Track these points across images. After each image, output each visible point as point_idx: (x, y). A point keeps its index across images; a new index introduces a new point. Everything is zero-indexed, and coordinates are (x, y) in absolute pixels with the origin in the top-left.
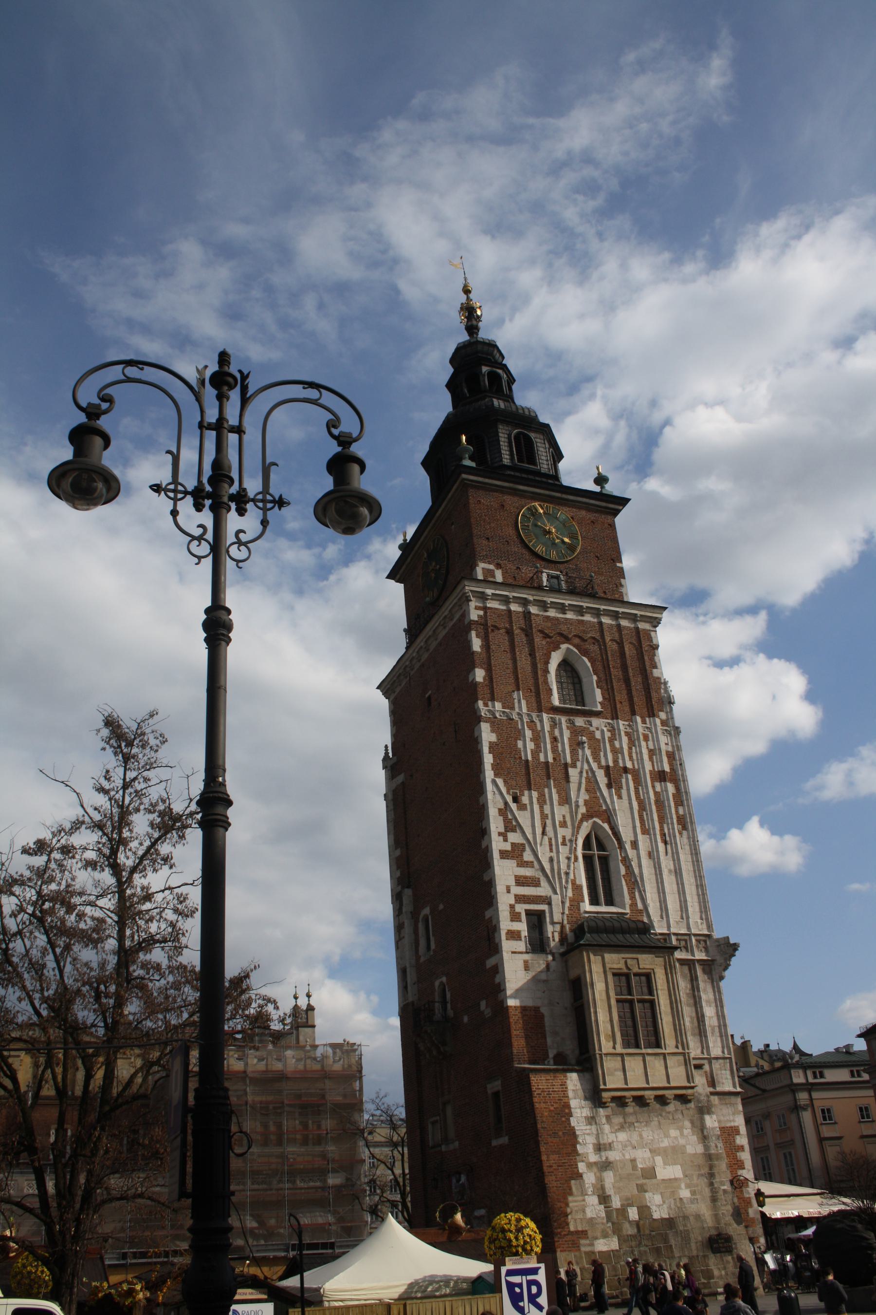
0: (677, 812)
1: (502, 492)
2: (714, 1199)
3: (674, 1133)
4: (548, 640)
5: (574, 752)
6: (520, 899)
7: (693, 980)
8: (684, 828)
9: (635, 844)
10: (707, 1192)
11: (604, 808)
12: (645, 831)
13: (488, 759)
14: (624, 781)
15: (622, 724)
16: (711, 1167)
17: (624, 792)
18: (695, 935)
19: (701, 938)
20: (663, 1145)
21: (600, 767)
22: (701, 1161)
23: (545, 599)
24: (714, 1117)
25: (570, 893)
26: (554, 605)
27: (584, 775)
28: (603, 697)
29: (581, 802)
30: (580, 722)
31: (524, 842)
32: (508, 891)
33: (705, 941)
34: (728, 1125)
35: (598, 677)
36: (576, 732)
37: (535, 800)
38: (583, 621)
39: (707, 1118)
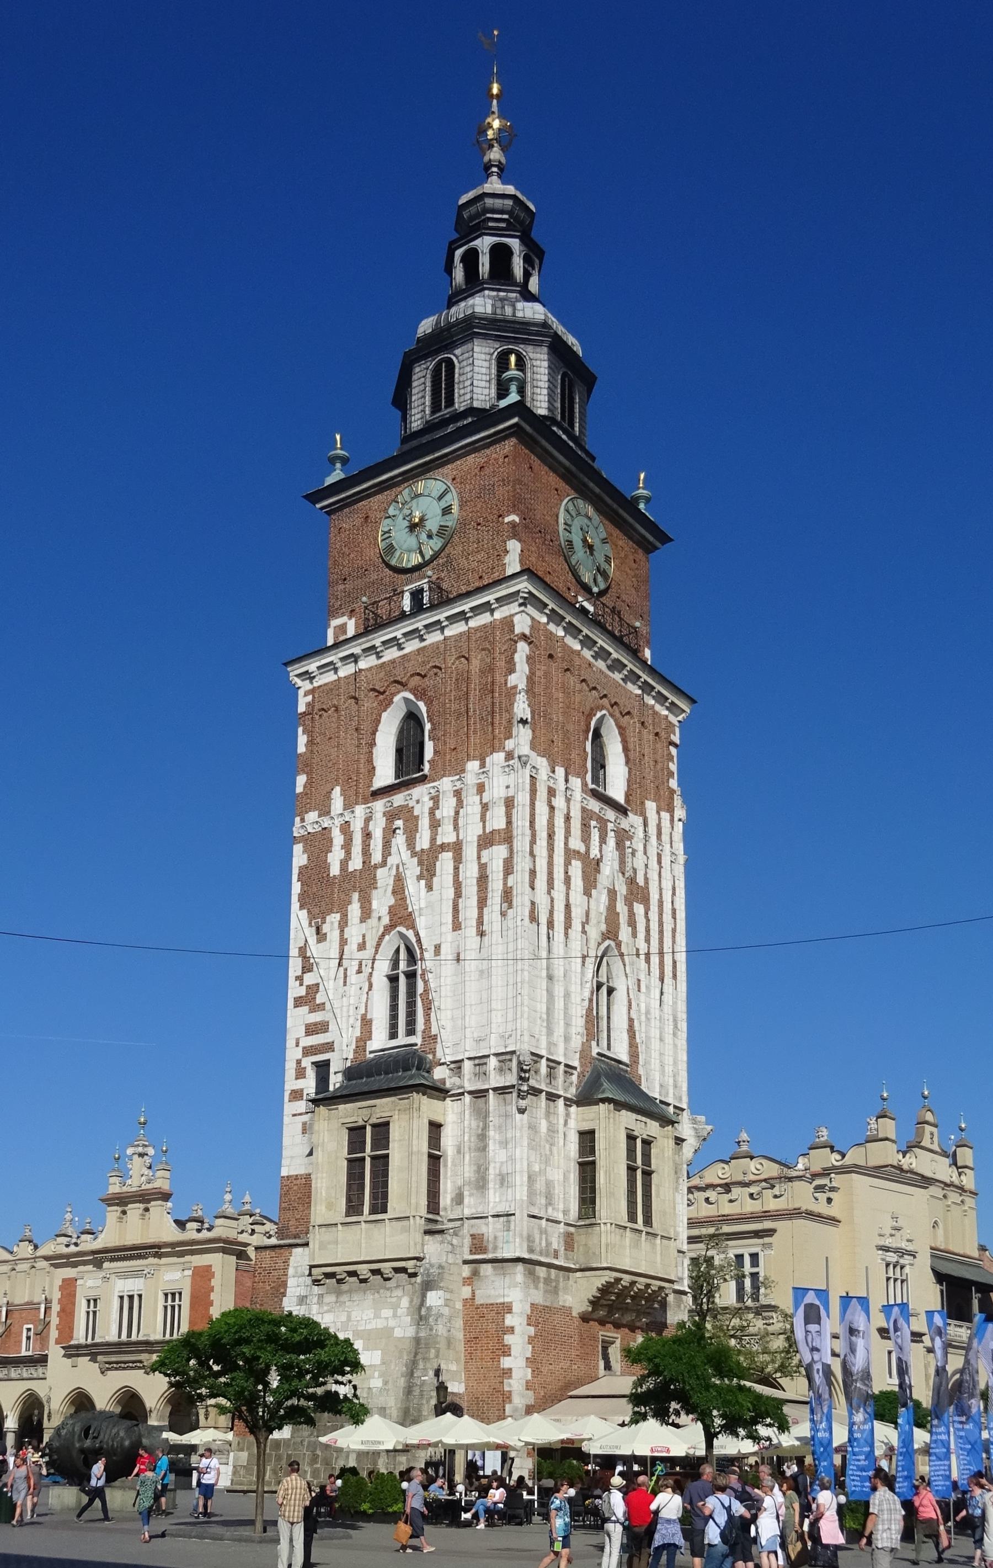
0: (505, 884)
1: (368, 496)
2: (409, 1391)
3: (387, 1313)
4: (381, 697)
5: (387, 845)
6: (308, 1051)
7: (483, 1115)
8: (510, 907)
9: (437, 949)
10: (402, 1382)
11: (410, 910)
12: (457, 926)
13: (296, 888)
14: (438, 864)
15: (446, 784)
16: (416, 1354)
17: (435, 879)
18: (496, 1055)
19: (503, 1057)
20: (369, 1327)
21: (414, 854)
22: (408, 1345)
23: (373, 643)
24: (440, 1293)
25: (359, 1034)
26: (477, 610)
27: (394, 872)
28: (436, 752)
29: (384, 911)
30: (399, 799)
31: (320, 981)
32: (297, 1046)
33: (511, 1060)
34: (499, 1301)
35: (433, 724)
36: (391, 816)
37: (336, 925)
38: (425, 647)
39: (429, 1294)
